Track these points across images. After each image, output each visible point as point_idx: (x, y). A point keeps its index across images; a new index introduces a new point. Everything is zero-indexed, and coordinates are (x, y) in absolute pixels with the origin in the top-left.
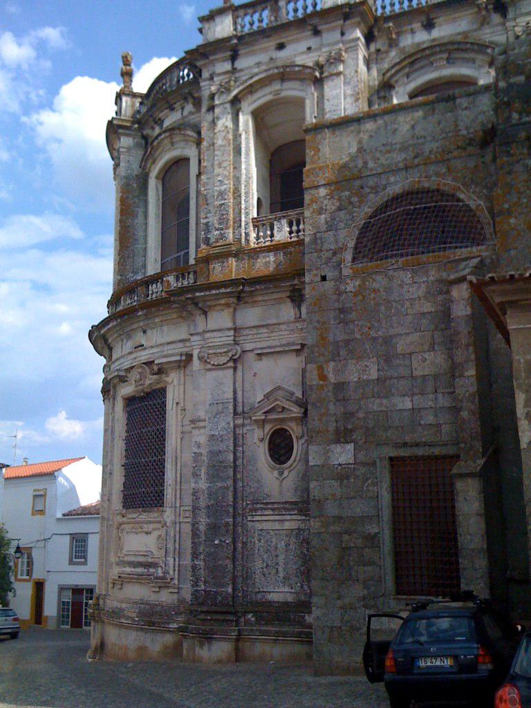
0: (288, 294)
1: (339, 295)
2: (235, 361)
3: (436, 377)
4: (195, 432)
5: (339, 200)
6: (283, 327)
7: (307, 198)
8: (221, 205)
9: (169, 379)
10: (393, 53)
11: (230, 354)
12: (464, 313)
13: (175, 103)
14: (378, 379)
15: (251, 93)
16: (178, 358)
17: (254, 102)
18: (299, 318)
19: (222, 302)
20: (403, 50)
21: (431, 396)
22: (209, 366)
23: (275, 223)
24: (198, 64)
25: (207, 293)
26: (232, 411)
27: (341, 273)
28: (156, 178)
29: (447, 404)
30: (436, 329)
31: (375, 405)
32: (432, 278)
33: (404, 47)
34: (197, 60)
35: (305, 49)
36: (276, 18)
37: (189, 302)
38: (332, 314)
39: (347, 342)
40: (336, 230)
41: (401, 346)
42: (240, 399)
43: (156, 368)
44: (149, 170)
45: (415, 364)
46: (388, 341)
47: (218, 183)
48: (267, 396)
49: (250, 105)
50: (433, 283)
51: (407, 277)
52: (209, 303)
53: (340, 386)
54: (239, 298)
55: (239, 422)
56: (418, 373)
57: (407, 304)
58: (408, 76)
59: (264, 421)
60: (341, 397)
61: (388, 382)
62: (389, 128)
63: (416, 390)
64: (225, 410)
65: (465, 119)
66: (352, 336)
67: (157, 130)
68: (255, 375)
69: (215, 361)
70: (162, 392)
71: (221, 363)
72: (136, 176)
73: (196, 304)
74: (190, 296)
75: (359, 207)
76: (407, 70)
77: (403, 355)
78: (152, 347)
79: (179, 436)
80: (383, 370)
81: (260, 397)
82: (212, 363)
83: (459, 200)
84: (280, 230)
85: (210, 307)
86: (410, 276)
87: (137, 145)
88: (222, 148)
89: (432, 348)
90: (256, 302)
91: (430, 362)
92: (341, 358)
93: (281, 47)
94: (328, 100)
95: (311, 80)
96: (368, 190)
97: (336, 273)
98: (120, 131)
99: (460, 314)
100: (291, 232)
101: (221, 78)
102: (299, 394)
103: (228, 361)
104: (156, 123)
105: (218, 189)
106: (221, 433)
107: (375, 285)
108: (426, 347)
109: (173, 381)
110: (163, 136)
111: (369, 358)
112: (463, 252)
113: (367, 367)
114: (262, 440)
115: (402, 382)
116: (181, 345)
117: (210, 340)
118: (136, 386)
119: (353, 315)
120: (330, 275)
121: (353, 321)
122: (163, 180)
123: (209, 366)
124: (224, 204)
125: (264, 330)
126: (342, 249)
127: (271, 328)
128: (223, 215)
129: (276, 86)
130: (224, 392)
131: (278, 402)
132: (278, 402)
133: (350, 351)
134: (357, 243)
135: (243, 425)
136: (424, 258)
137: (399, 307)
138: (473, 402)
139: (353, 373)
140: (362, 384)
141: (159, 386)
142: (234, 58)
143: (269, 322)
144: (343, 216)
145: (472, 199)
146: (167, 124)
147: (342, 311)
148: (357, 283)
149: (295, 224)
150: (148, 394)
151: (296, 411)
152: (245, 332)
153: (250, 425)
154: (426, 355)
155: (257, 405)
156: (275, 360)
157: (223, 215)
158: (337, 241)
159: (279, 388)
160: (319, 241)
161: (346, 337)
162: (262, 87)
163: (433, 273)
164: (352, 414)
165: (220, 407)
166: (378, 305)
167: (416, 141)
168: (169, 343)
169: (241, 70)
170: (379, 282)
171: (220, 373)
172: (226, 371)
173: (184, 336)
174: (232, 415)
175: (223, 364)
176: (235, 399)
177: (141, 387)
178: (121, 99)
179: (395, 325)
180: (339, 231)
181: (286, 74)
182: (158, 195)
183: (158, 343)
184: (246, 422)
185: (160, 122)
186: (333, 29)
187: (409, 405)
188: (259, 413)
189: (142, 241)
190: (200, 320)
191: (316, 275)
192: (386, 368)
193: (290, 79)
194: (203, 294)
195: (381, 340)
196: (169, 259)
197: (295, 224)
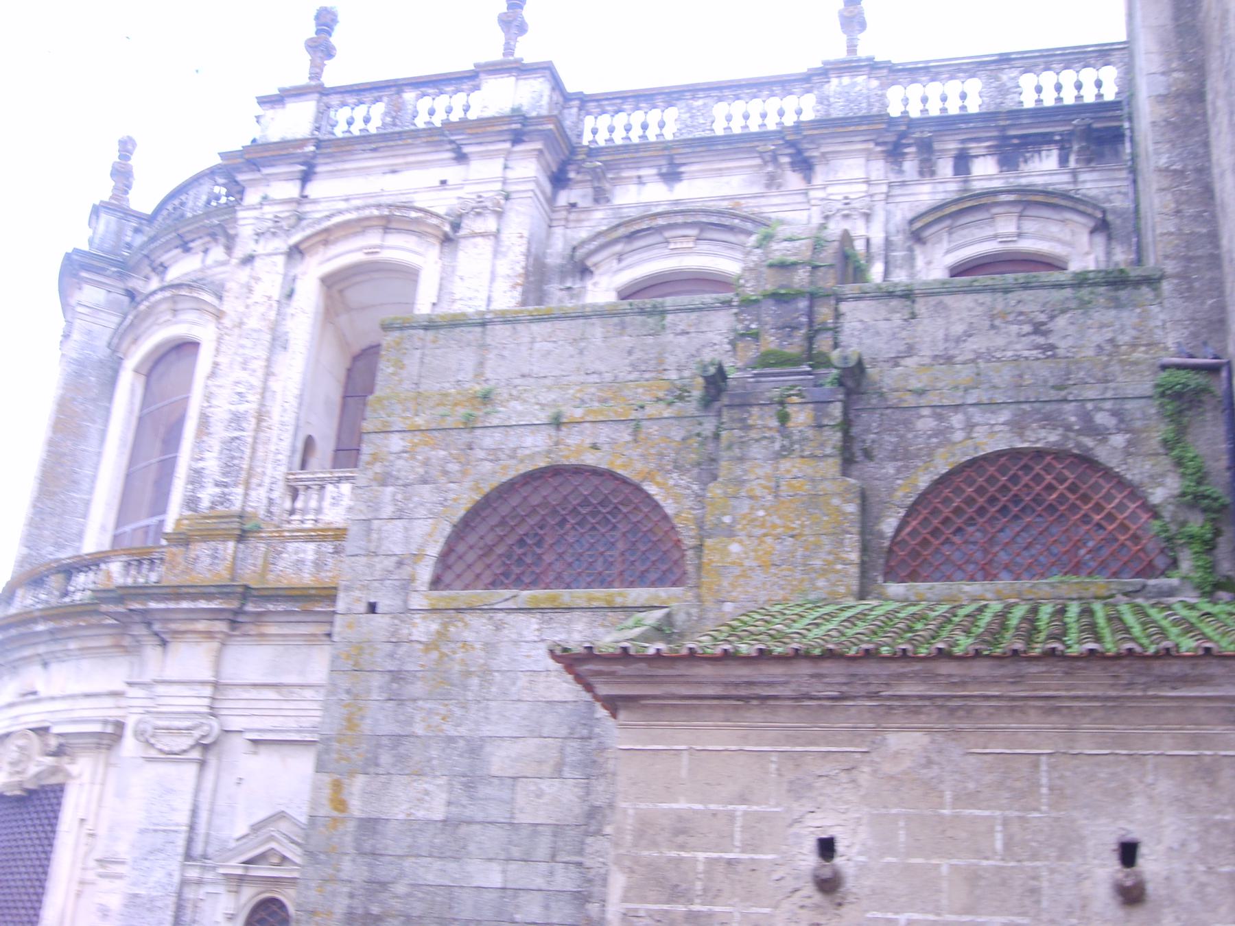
1: (397, 643)
2: (206, 748)
3: (558, 829)
4: (105, 884)
5: (426, 463)
7: (366, 449)
9: (74, 769)
10: (599, 215)
11: (197, 733)
13: (193, 241)
14: (444, 821)
15: (326, 243)
16: (97, 728)
17: (329, 260)
19: (201, 626)
22: (153, 753)
24: (241, 177)
26: (181, 849)
27: (405, 602)
28: (136, 371)
29: (570, 887)
31: (431, 873)
33: (620, 207)
35: (438, 184)
37: (137, 618)
38: (377, 681)
39: (397, 739)
41: (499, 760)
42: (202, 829)
43: (53, 743)
44: (125, 354)
45: (521, 800)
46: (475, 748)
48: (256, 828)
49: (321, 263)
52: (173, 626)
53: (370, 825)
54: (233, 623)
55: (193, 874)
56: (523, 818)
58: (620, 257)
59: (241, 880)
60: (367, 847)
62: (537, 346)
65: (678, 351)
66: (407, 730)
67: (155, 284)
68: (240, 782)
70: (57, 791)
71: (176, 749)
72: (101, 361)
73: (149, 624)
76: (618, 248)
78: (53, 698)
79: (75, 887)
81: (241, 829)
84: (336, 501)
86: (536, 626)
87: (111, 306)
89: (558, 773)
90: (263, 635)
92: (380, 770)
95: (436, 236)
96: (481, 454)
98: (84, 274)
101: (277, 208)
103: (193, 747)
104: (154, 270)
105: (233, 408)
107: (468, 635)
108: (547, 769)
109: (80, 775)
110: (159, 296)
111: (435, 777)
112: (638, 595)
113: (427, 793)
114: (231, 918)
116: (109, 702)
118: (11, 774)
119: (417, 688)
122: (148, 376)
123: (153, 753)
124: (237, 438)
126: (418, 557)
127: (284, 690)
128: (233, 458)
129: (373, 238)
130: (173, 810)
132: (273, 845)
133: (401, 759)
135: (200, 882)
140: (413, 826)
141: (53, 780)
142: (306, 178)
146: (173, 275)
150: (31, 792)
153: (213, 883)
154: (544, 785)
155: (233, 844)
157: (233, 458)
159: (281, 816)
160: (375, 536)
161: (398, 730)
162: (346, 237)
164: (384, 885)
165: (159, 839)
166: (468, 674)
167: (582, 378)
168: (87, 696)
169: (315, 202)
170: (475, 629)
173: (119, 686)
174: (180, 858)
175: (184, 751)
176: (192, 827)
177: (16, 778)
178: (98, 217)
182: (131, 403)
183: (68, 692)
184: (209, 876)
185: (162, 269)
188: (233, 863)
189: (85, 486)
190: (152, 653)
191: (359, 600)
192: (464, 801)
193: (399, 230)
196: (128, 528)
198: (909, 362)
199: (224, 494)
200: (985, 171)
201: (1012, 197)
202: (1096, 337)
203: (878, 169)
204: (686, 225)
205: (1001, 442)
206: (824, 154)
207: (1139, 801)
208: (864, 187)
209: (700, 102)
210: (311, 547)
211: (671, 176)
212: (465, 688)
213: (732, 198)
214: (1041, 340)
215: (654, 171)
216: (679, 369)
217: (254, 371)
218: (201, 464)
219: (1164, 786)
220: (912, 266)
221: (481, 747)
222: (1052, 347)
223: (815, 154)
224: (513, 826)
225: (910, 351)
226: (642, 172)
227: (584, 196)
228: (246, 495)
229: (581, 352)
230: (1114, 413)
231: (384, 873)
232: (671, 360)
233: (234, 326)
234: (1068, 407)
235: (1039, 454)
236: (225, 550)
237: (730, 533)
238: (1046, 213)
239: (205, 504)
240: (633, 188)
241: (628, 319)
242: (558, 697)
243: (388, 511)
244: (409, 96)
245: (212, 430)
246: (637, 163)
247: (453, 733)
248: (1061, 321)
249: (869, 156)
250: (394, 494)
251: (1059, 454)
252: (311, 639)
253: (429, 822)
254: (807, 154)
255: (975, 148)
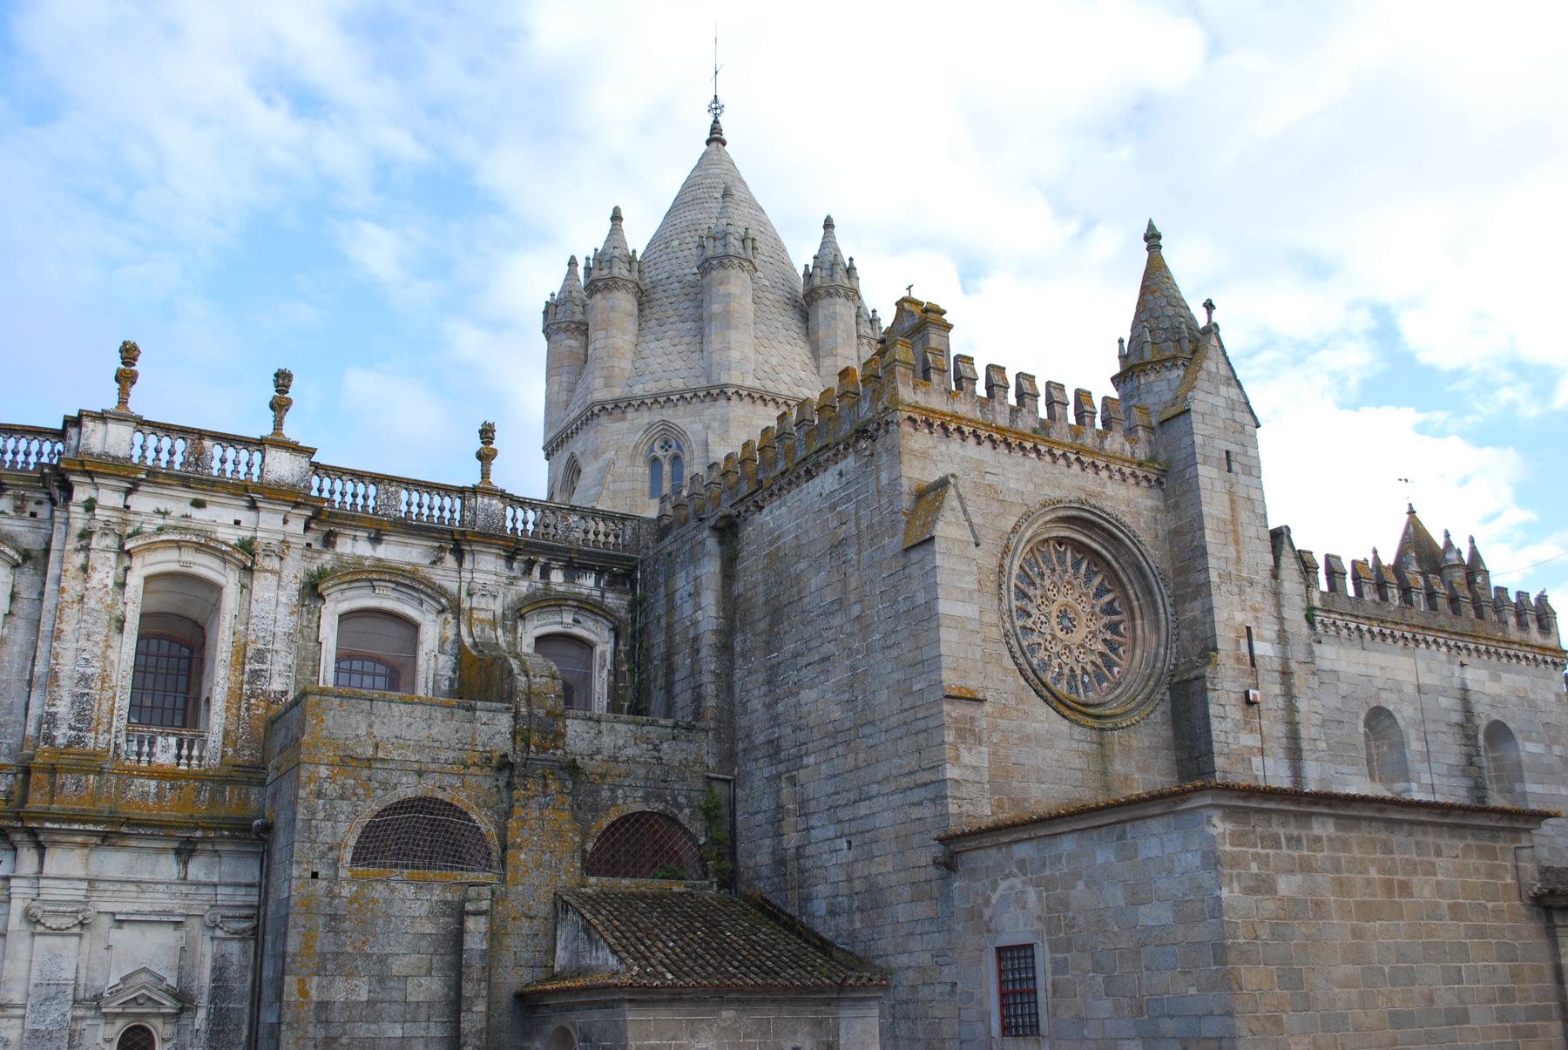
0: (176, 845)
1: (333, 898)
3: (430, 1004)
6: (161, 888)
7: (304, 774)
8: (83, 695)
12: (479, 947)
14: (368, 1001)
18: (184, 880)
19: (79, 839)
20: (339, 556)
21: (423, 1024)
22: (40, 928)
23: (159, 739)
24: (73, 478)
25: (64, 827)
26: (71, 997)
27: (336, 873)
29: (438, 1035)
30: (435, 953)
31: (362, 1030)
32: (435, 898)
33: (342, 555)
34: (73, 472)
36: (197, 459)
38: (321, 920)
39: (337, 955)
40: (336, 822)
41: (397, 966)
42: (82, 981)
45: (409, 990)
46: (383, 960)
47: (83, 662)
48: (124, 980)
49: (144, 566)
50: (437, 902)
51: (408, 891)
53: (323, 1006)
56: (410, 999)
57: (408, 922)
59: (117, 1015)
60: (323, 1018)
61: (379, 1005)
63: (408, 1017)
64: (60, 995)
66: (344, 949)
68: (109, 947)
69: (52, 922)
71: (63, 927)
74: (35, 825)
75: (364, 801)
77: (398, 977)
80: (374, 992)
81: (114, 980)
82: (48, 925)
83: (470, 820)
84: (165, 749)
85: (55, 843)
88: (95, 614)
89: (429, 973)
91: (427, 988)
93: (198, 504)
94: (257, 601)
95: (238, 566)
97: (331, 872)
99: (474, 946)
100: (179, 757)
102: (172, 982)
103: (74, 926)
105: (81, 670)
106: (50, 1028)
115: (395, 1007)
117: (48, 891)
119: (347, 925)
120: (322, 873)
121: (345, 932)
124: (88, 694)
125: (133, 888)
127: (143, 886)
129: (188, 556)
131: (144, 991)
132: (144, 991)
133: (339, 966)
134: (358, 842)
135: (83, 1018)
136: (430, 874)
137: (399, 922)
138: (479, 1038)
139: (339, 992)
140: (348, 1005)
142: (128, 492)
143: (139, 877)
144: (345, 807)
145: (484, 822)
147: (333, 917)
148: (355, 888)
149: (185, 746)
151: (169, 1006)
152: (102, 886)
153: (93, 1018)
156: (143, 932)
158: (334, 834)
159: (144, 970)
161: (333, 948)
163: (437, 892)
164: (335, 1040)
165: (53, 991)
170: (380, 891)
171: (58, 941)
172: (68, 939)
174: (71, 1003)
179: (392, 943)
180: (339, 824)
181: (207, 545)
186: (275, 512)
187: (399, 1033)
188: (114, 1004)
194: (57, 826)
195: (375, 957)
197: (185, 746)
198: (599, 757)
199: (80, 737)
200: (557, 577)
201: (575, 603)
202: (680, 757)
203: (500, 565)
204: (389, 581)
205: (639, 807)
206: (472, 551)
207: (799, 1034)
208: (494, 578)
209: (393, 489)
210: (153, 783)
211: (376, 540)
212: (376, 925)
213: (414, 565)
214: (656, 754)
215: (366, 535)
216: (484, 746)
217: (98, 643)
218: (53, 709)
219: (807, 1029)
220: (516, 632)
221: (387, 959)
222: (661, 758)
223: (468, 548)
224: (407, 1003)
225: (598, 752)
226: (358, 533)
227: (316, 540)
228: (96, 738)
229: (430, 727)
230: (686, 797)
231: (334, 1032)
232: (479, 740)
233: (73, 602)
234: (668, 792)
235: (652, 814)
236: (87, 780)
237: (520, 848)
238: (589, 615)
239: (61, 741)
240: (349, 541)
241: (455, 710)
242: (427, 931)
243: (321, 815)
244: (207, 443)
245: (61, 683)
246: (356, 528)
247: (369, 951)
248: (665, 746)
249: (498, 556)
250: (324, 805)
251: (661, 814)
252: (163, 850)
253: (358, 1003)
254: (463, 547)
255: (554, 564)
